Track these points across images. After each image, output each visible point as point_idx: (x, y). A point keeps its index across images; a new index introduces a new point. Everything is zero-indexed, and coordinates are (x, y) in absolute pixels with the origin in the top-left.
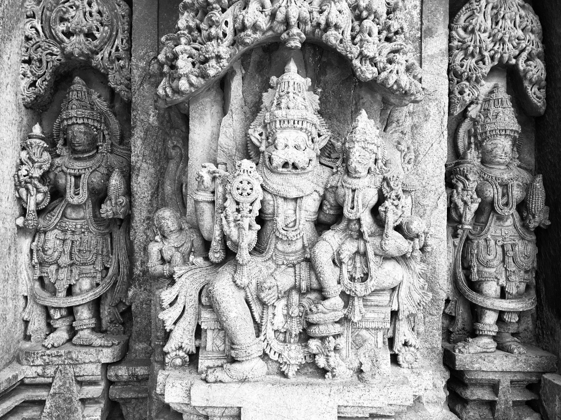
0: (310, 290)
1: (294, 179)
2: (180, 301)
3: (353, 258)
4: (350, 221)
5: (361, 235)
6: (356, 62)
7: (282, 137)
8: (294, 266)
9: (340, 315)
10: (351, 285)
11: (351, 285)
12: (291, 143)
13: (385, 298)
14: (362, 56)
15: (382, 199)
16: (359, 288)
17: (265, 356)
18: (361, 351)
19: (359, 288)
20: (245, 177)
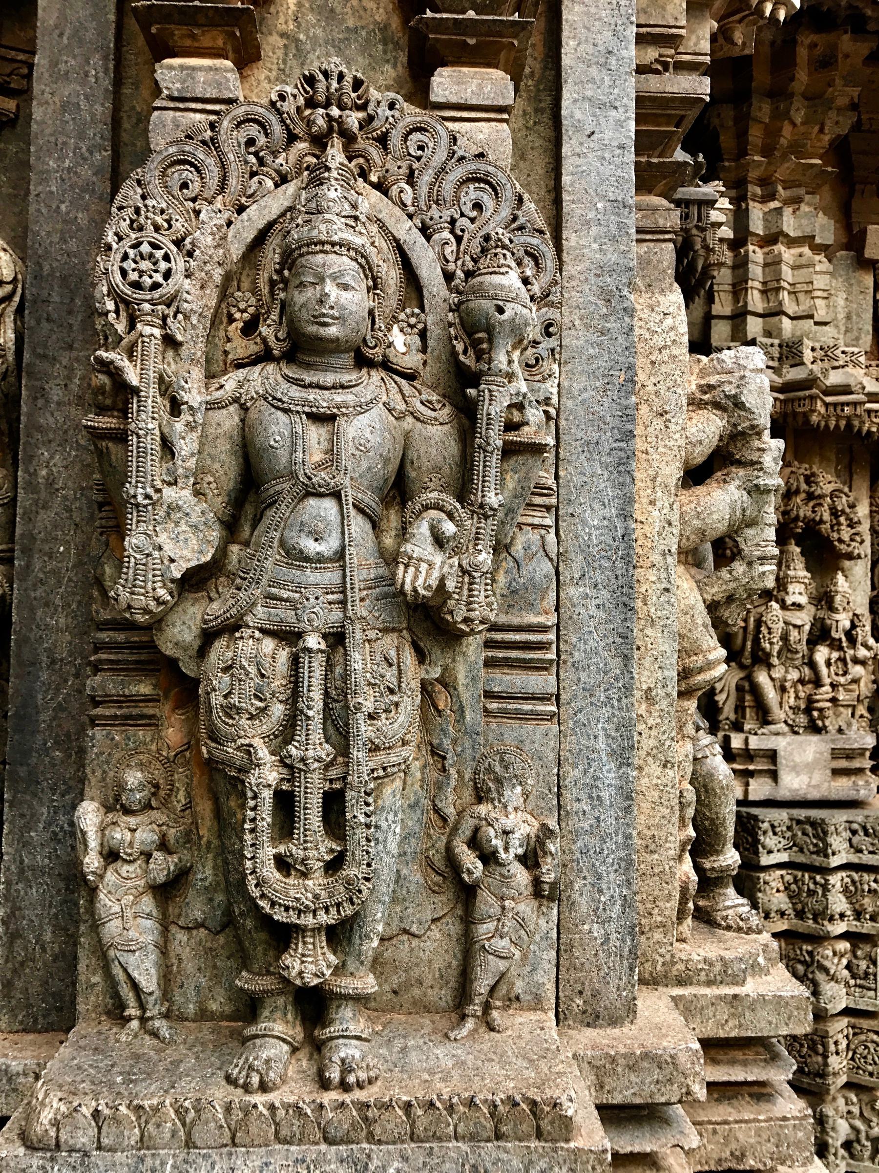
0: (809, 682)
1: (798, 613)
2: (726, 689)
3: (836, 662)
4: (834, 639)
5: (840, 648)
6: (836, 543)
7: (791, 588)
8: (797, 668)
9: (830, 696)
10: (836, 678)
11: (836, 678)
12: (797, 591)
13: (854, 686)
14: (840, 541)
15: (853, 626)
16: (842, 680)
17: (786, 722)
18: (839, 719)
19: (842, 680)
20: (774, 613)
